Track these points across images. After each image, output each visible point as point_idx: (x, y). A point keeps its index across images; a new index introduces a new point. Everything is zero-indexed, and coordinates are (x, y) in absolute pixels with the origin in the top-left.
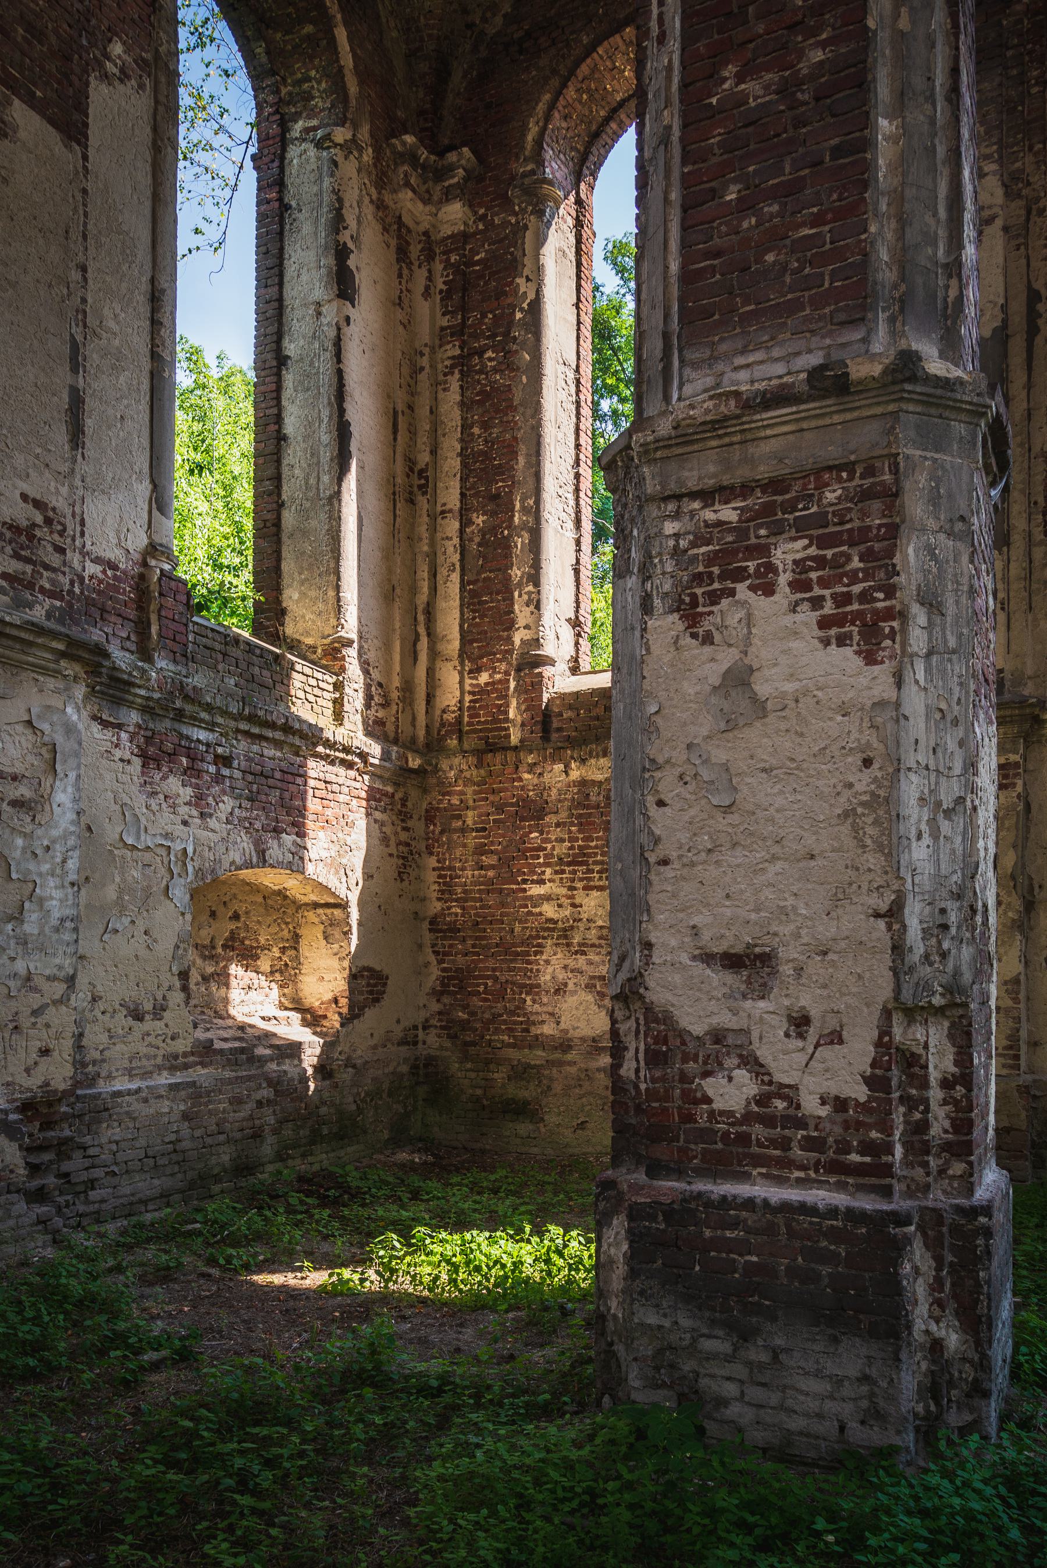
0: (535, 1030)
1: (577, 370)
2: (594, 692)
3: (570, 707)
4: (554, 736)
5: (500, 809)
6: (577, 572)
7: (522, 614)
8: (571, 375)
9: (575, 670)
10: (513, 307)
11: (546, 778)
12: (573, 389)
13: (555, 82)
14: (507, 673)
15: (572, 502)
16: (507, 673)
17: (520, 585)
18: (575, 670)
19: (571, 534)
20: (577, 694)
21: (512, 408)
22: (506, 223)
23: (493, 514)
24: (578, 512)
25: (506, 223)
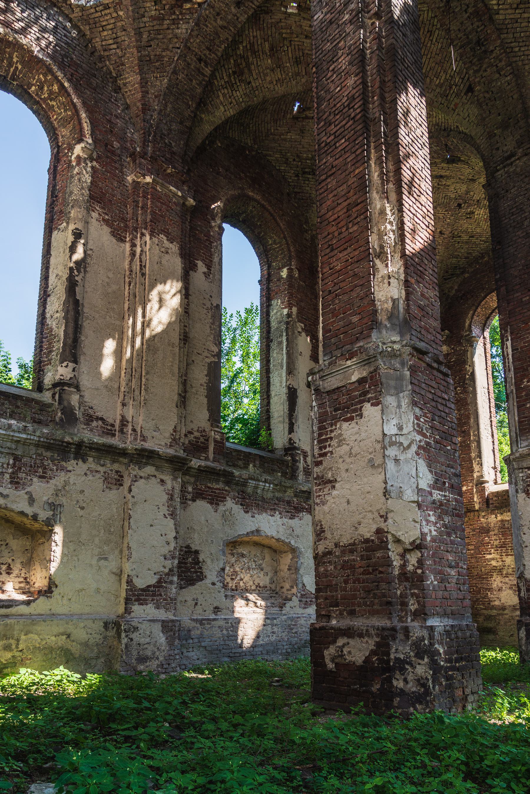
0: (492, 604)
1: (488, 389)
2: (503, 491)
3: (496, 496)
4: (491, 506)
5: (474, 530)
6: (494, 451)
7: (476, 467)
8: (486, 391)
9: (496, 483)
11: (489, 520)
13: (474, 308)
14: (472, 486)
15: (490, 430)
16: (472, 486)
17: (475, 458)
18: (496, 483)
19: (490, 440)
20: (498, 492)
21: (467, 404)
22: (461, 350)
23: (464, 437)
24: (492, 433)
25: (461, 350)
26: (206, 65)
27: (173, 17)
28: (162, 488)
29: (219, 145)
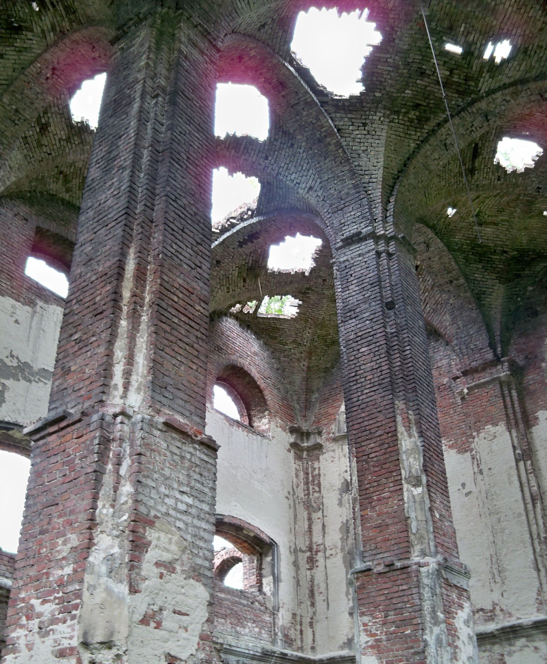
26: (458, 280)
27: (421, 280)
28: (538, 655)
29: (531, 288)
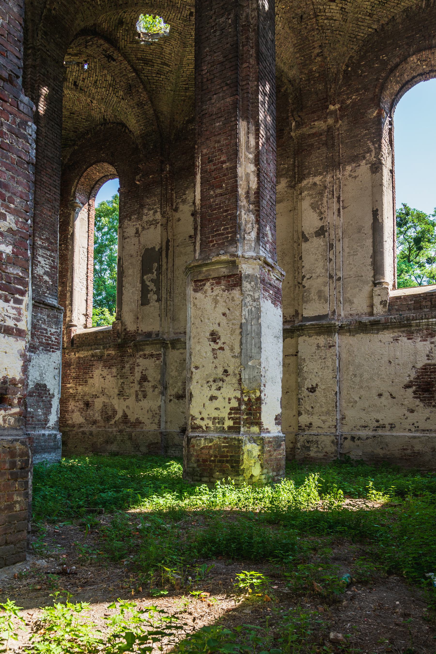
0: (67, 422)
4: (75, 345)
6: (87, 301)
8: (86, 250)
9: (86, 327)
10: (68, 234)
11: (71, 356)
12: (86, 254)
13: (78, 177)
18: (86, 327)
21: (67, 260)
23: (63, 287)
24: (87, 286)
25: (67, 212)
